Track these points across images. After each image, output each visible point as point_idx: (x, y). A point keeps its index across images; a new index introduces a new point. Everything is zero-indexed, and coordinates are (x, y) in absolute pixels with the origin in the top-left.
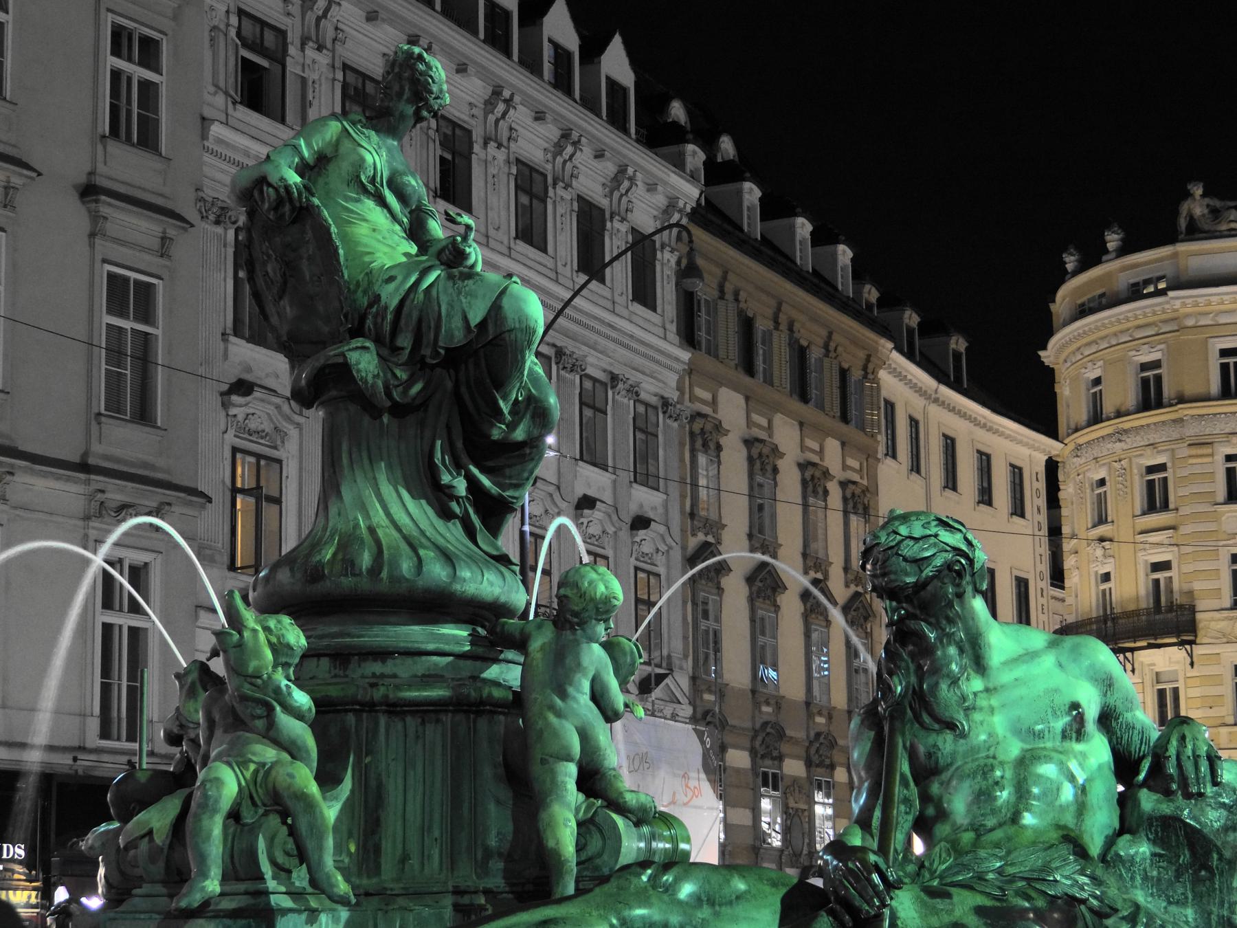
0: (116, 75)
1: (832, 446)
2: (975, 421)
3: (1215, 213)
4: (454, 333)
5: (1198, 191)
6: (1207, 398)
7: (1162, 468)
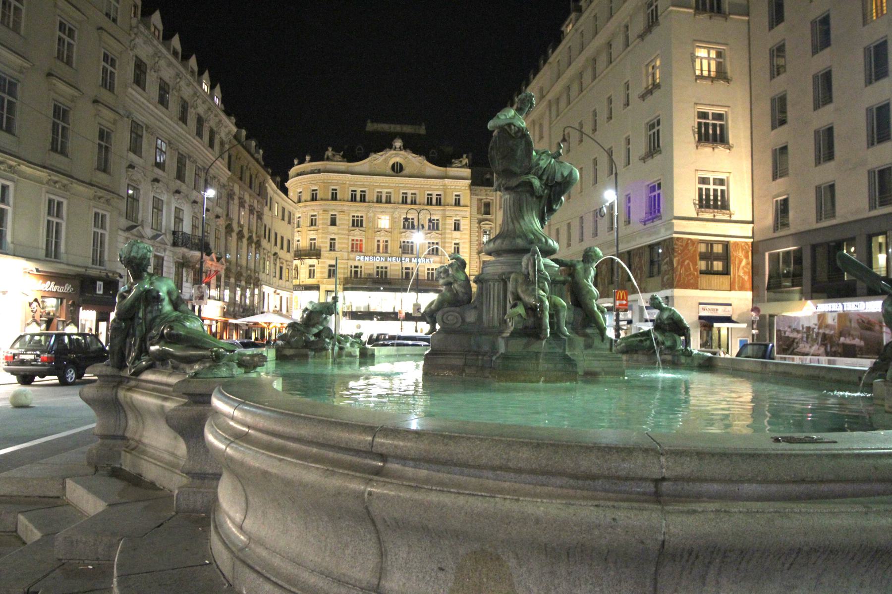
0: (104, 67)
1: (256, 201)
2: (283, 199)
3: (334, 155)
4: (558, 178)
5: (330, 149)
6: (328, 200)
7: (315, 216)
